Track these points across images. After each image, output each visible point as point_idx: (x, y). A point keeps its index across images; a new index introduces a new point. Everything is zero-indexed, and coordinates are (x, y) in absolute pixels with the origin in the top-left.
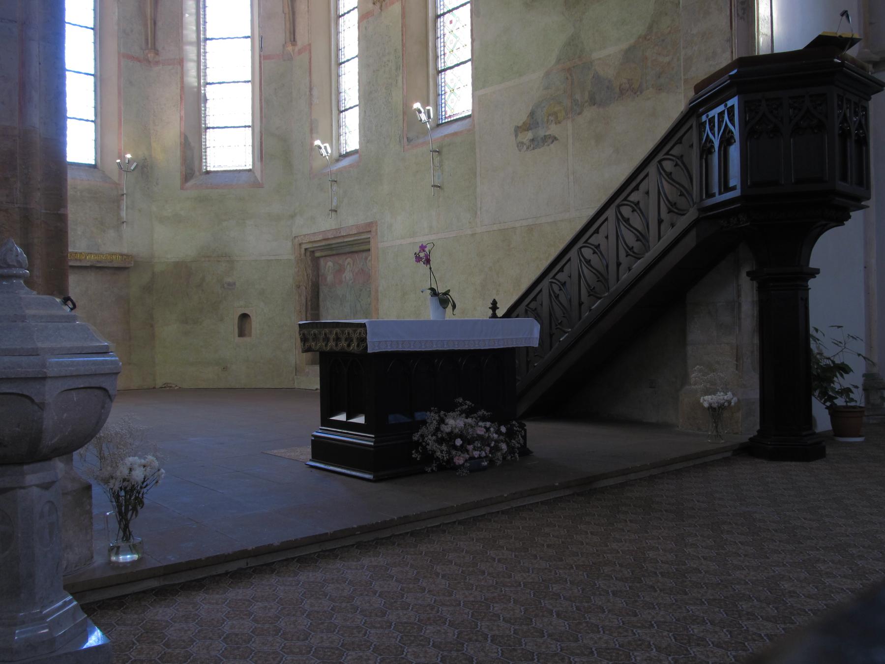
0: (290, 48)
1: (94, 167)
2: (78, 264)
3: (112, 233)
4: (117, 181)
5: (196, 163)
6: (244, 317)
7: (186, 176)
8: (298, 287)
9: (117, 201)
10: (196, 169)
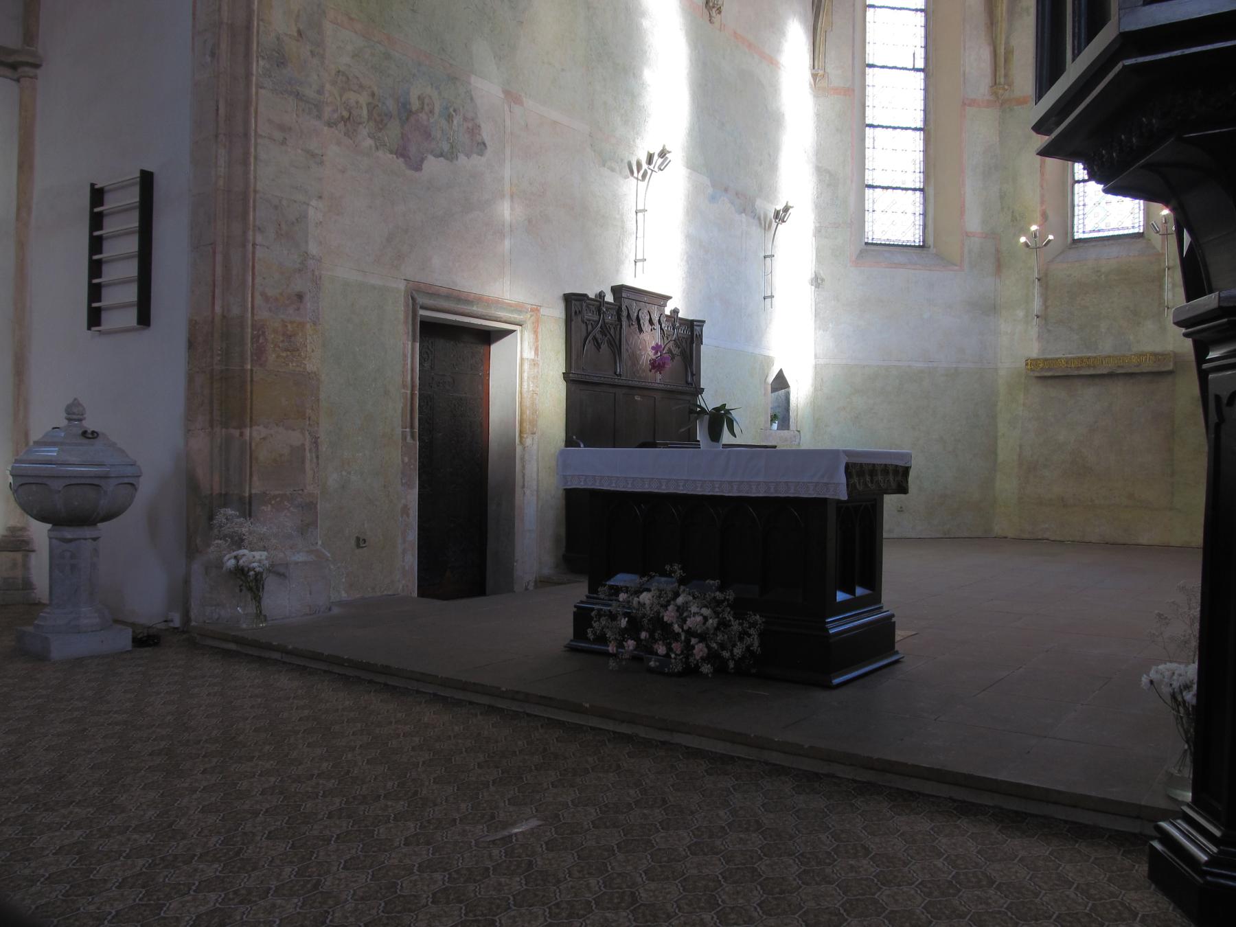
2: (1091, 372)
3: (1150, 325)
4: (1161, 252)
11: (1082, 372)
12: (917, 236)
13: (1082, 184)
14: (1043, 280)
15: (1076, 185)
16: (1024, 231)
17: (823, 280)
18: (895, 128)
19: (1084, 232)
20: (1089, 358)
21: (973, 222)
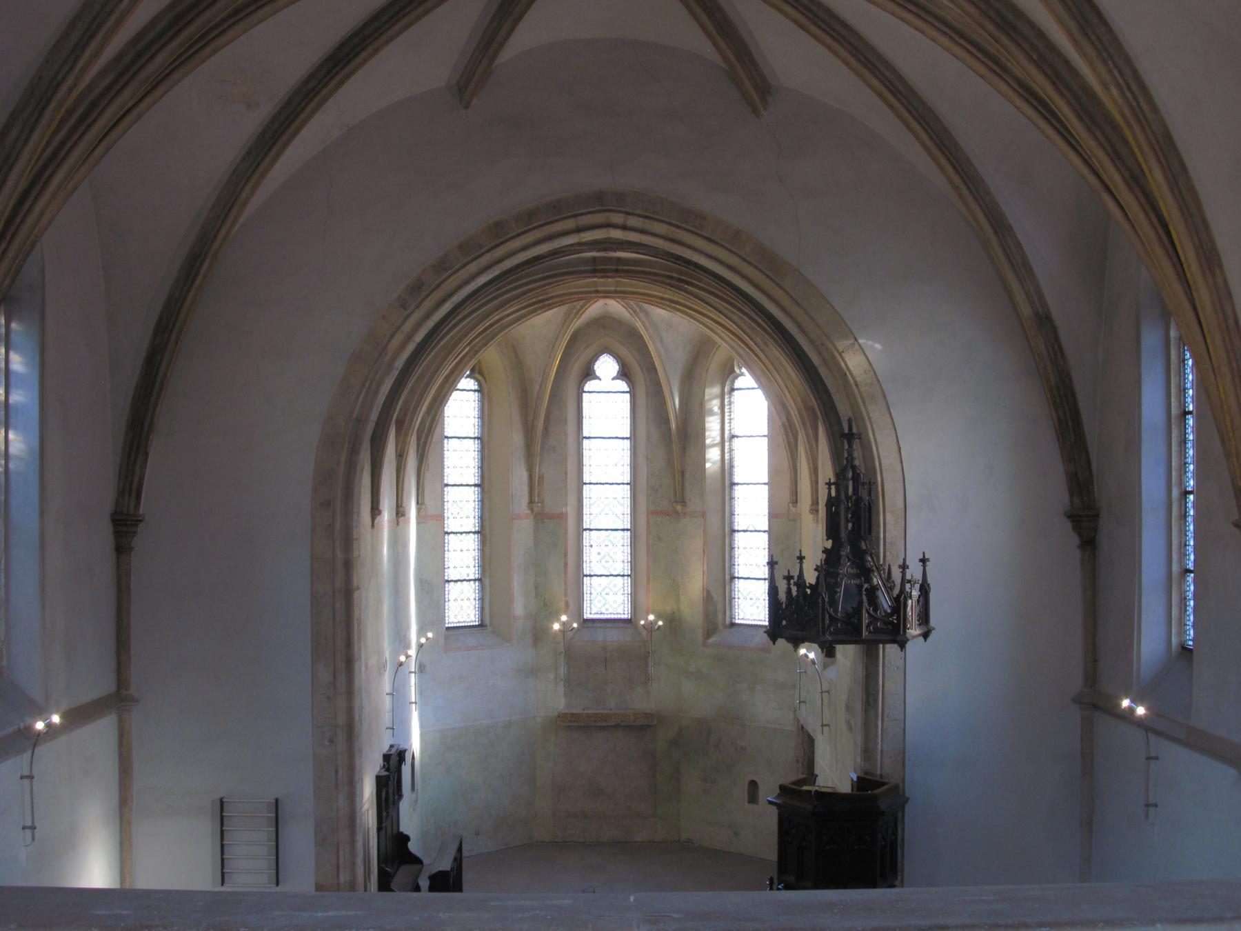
2: (604, 724)
5: (720, 616)
6: (753, 785)
7: (708, 632)
9: (644, 658)
10: (720, 623)
11: (599, 724)
12: (477, 616)
13: (588, 578)
15: (585, 578)
17: (424, 666)
19: (591, 613)
20: (602, 714)
21: (519, 608)
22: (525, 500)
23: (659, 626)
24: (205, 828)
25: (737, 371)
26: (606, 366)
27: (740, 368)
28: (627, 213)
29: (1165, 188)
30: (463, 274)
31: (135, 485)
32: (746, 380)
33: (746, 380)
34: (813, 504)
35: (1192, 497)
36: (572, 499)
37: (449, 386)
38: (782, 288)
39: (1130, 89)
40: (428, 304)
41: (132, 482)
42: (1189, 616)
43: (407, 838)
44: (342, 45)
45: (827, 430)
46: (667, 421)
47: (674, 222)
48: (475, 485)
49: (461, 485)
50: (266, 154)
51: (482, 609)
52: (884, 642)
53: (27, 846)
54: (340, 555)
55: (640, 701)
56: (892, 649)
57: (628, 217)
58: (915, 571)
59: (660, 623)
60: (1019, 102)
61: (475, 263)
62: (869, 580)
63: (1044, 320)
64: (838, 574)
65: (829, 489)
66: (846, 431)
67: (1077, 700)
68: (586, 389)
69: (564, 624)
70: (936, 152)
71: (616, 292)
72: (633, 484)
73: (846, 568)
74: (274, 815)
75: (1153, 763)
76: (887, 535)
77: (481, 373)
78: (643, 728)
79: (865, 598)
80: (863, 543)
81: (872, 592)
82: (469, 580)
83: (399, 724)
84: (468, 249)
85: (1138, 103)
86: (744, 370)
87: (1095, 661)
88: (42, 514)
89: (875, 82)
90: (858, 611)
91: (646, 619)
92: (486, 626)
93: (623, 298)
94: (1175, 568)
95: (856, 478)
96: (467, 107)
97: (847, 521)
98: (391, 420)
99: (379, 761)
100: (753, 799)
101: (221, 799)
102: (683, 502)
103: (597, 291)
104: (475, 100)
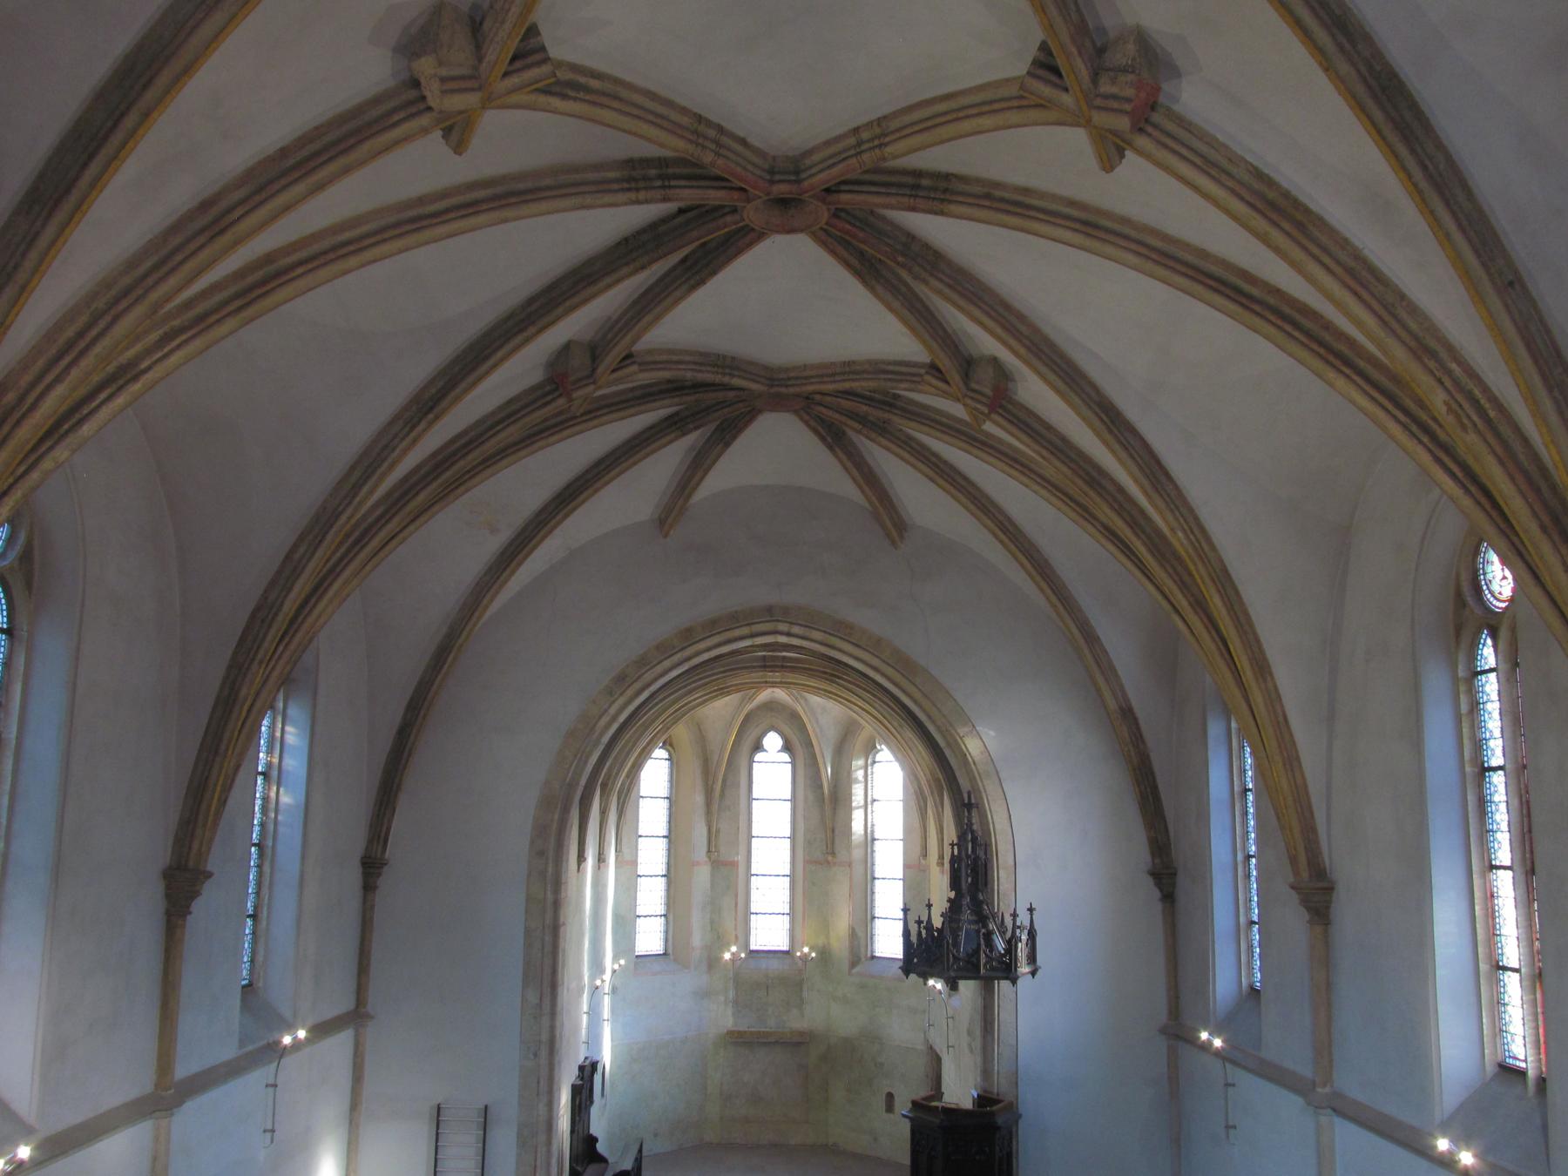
0: (923, 861)
1: (787, 952)
2: (765, 1041)
5: (863, 950)
6: (890, 1096)
8: (927, 1076)
10: (862, 956)
14: (738, 981)
16: (729, 950)
18: (651, 876)
21: (697, 939)
22: (705, 849)
23: (812, 958)
24: (421, 1134)
25: (878, 747)
26: (773, 741)
27: (880, 745)
28: (791, 623)
29: (1224, 612)
30: (659, 669)
31: (383, 835)
32: (885, 754)
33: (885, 754)
34: (939, 858)
35: (1254, 860)
36: (742, 848)
37: (645, 754)
38: (914, 684)
39: (1192, 532)
40: (630, 692)
41: (381, 831)
42: (1256, 961)
43: (595, 1140)
44: (568, 486)
45: (951, 799)
46: (821, 787)
47: (828, 631)
48: (664, 837)
49: (653, 836)
50: (505, 569)
51: (666, 941)
52: (999, 979)
53: (267, 1147)
54: (550, 896)
55: (796, 1022)
56: (1005, 985)
57: (793, 626)
58: (1024, 919)
59: (813, 955)
60: (1103, 541)
61: (669, 660)
62: (985, 926)
63: (1127, 713)
64: (960, 920)
65: (953, 849)
66: (966, 801)
67: (1163, 1031)
68: (756, 759)
69: (733, 954)
70: (1038, 578)
71: (781, 683)
72: (793, 838)
73: (967, 915)
74: (483, 1120)
75: (1230, 1089)
76: (1001, 887)
77: (671, 745)
78: (798, 1044)
79: (982, 940)
80: (980, 894)
81: (988, 936)
82: (656, 916)
83: (594, 1039)
84: (664, 649)
85: (1200, 544)
86: (883, 746)
87: (1177, 997)
88: (303, 857)
89: (989, 522)
90: (977, 952)
91: (802, 952)
92: (669, 955)
93: (788, 688)
94: (1242, 919)
95: (974, 840)
96: (666, 536)
97: (968, 876)
98: (597, 785)
99: (576, 1072)
100: (890, 1108)
101: (439, 1105)
102: (833, 854)
103: (766, 682)
104: (672, 532)
